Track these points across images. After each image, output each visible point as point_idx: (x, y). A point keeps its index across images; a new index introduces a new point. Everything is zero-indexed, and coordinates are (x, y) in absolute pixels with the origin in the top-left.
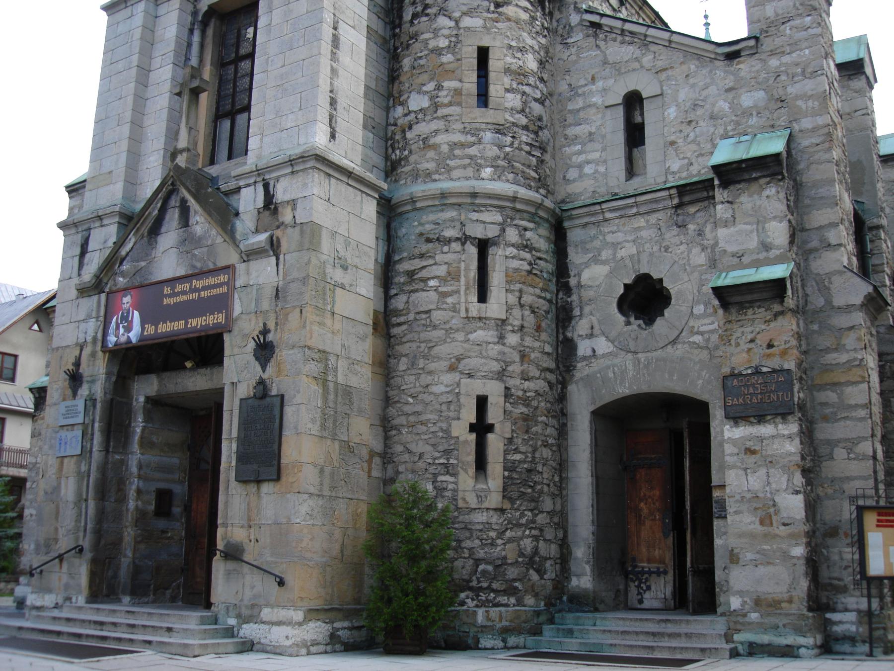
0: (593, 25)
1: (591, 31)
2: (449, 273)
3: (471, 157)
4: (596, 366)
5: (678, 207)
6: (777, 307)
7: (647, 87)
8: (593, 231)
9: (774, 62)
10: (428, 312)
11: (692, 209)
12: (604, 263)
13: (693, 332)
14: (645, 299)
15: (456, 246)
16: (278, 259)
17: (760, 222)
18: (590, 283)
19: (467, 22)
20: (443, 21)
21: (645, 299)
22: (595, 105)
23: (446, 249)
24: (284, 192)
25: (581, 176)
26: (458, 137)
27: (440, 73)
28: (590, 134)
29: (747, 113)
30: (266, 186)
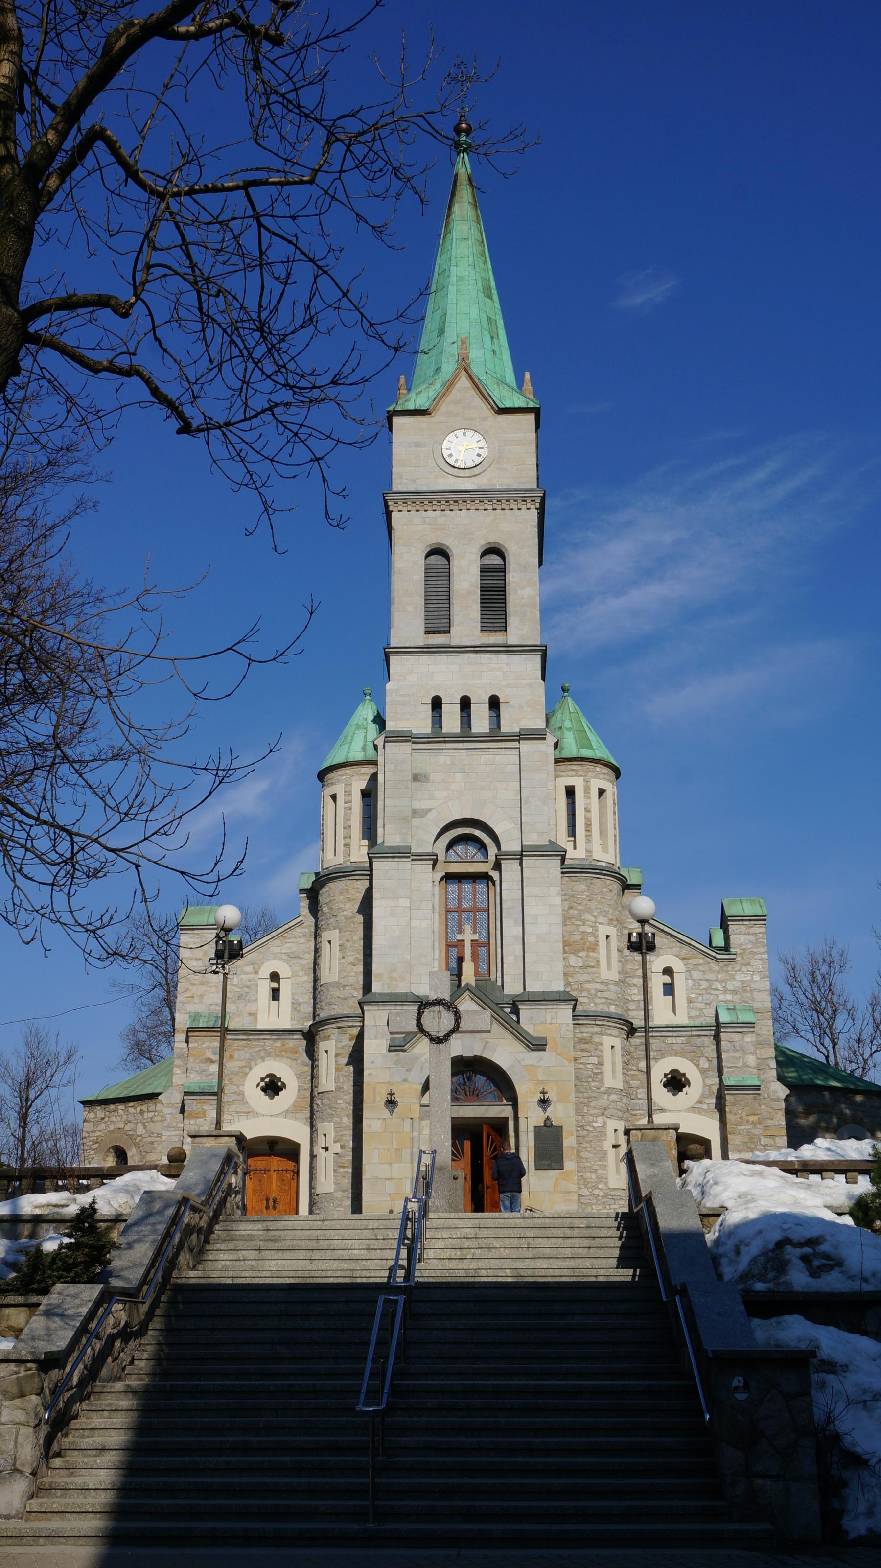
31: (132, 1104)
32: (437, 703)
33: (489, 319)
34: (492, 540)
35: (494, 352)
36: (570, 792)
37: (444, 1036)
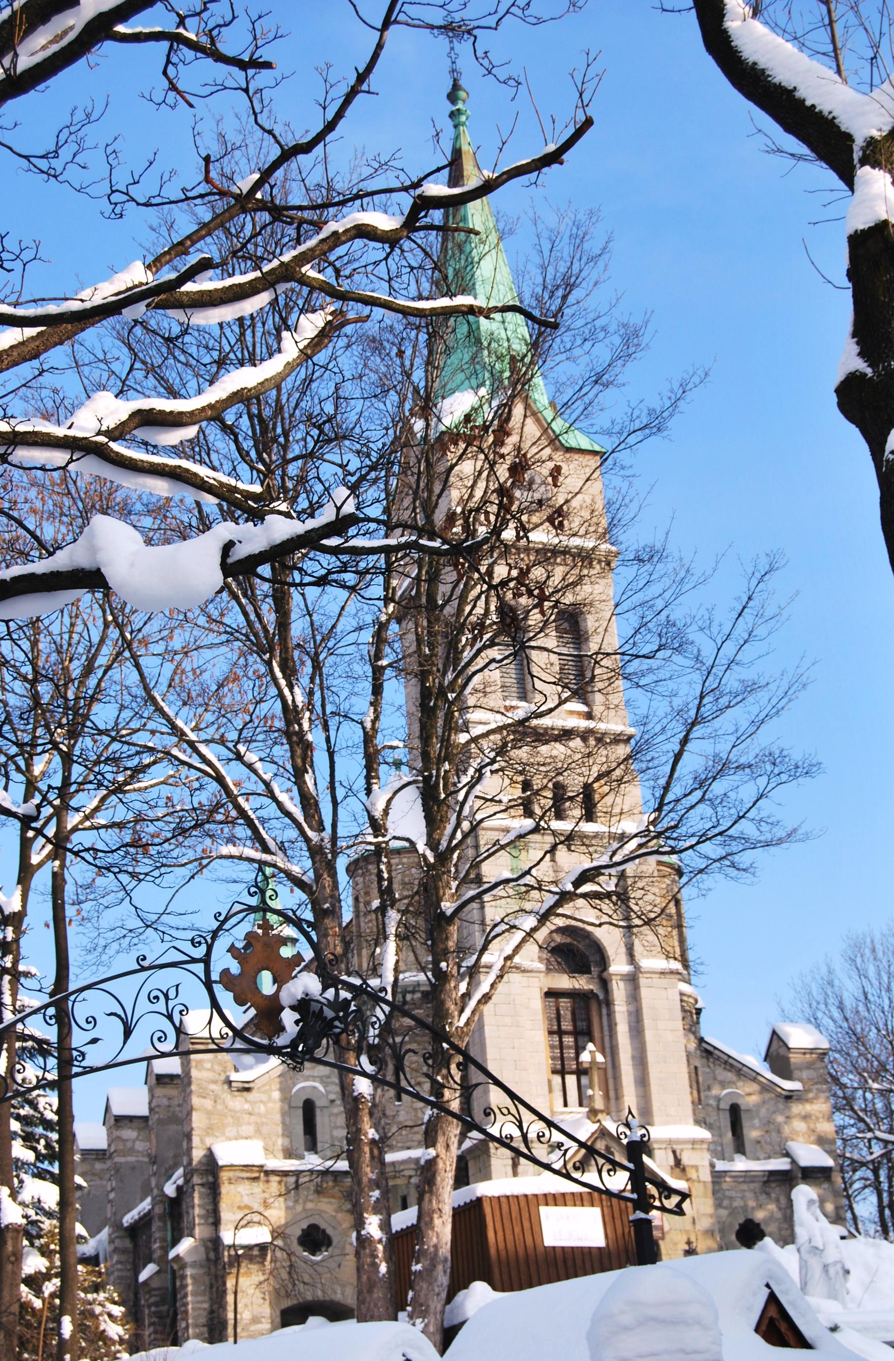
0: (706, 1051)
5: (765, 1182)
11: (773, 1185)
12: (726, 1208)
22: (710, 1105)
30: (674, 1152)
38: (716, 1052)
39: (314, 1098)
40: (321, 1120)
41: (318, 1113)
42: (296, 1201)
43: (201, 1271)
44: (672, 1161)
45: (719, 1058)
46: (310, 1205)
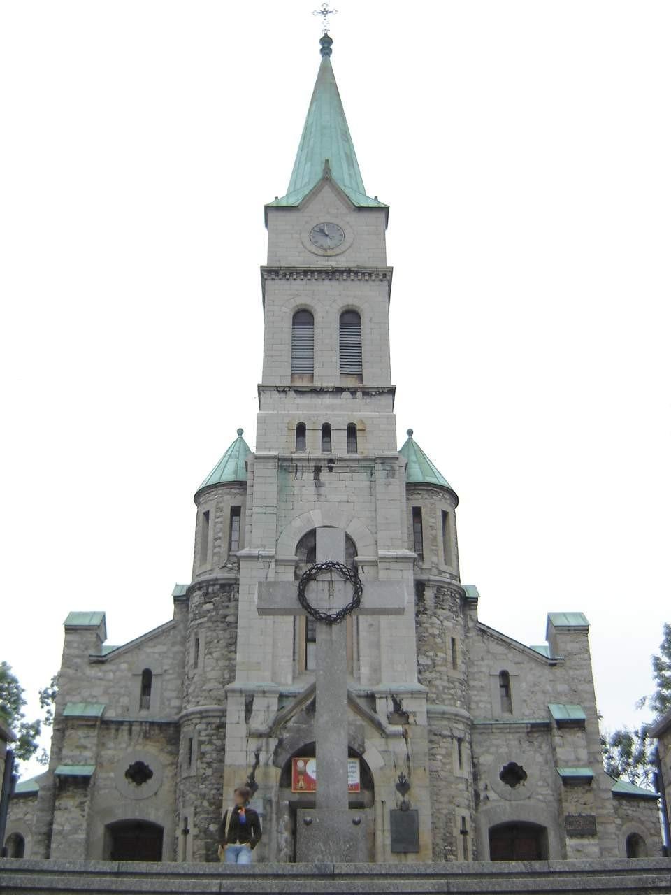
1: (479, 633)
2: (447, 753)
3: (452, 695)
4: (489, 805)
5: (528, 733)
6: (587, 787)
7: (512, 671)
8: (486, 737)
9: (571, 672)
10: (437, 771)
11: (536, 735)
12: (492, 754)
13: (538, 794)
14: (513, 774)
15: (449, 739)
16: (407, 740)
17: (576, 747)
18: (485, 763)
19: (446, 623)
20: (435, 620)
21: (513, 774)
23: (444, 740)
24: (407, 706)
25: (478, 707)
26: (446, 684)
27: (435, 648)
28: (482, 687)
29: (560, 694)
30: (395, 701)
31: (31, 798)
32: (301, 430)
33: (346, 153)
34: (351, 303)
35: (350, 175)
36: (417, 513)
37: (338, 615)
38: (488, 630)
39: (151, 668)
40: (155, 684)
41: (154, 679)
42: (129, 745)
43: (49, 793)
44: (391, 707)
45: (492, 636)
46: (138, 748)
